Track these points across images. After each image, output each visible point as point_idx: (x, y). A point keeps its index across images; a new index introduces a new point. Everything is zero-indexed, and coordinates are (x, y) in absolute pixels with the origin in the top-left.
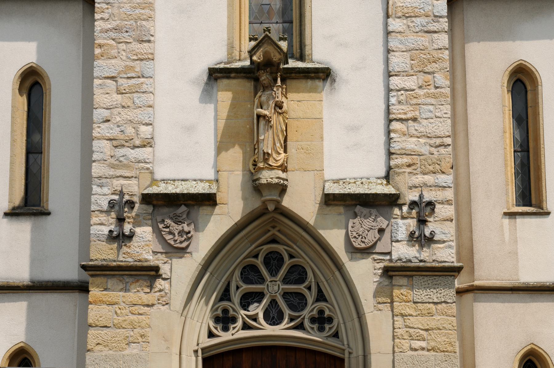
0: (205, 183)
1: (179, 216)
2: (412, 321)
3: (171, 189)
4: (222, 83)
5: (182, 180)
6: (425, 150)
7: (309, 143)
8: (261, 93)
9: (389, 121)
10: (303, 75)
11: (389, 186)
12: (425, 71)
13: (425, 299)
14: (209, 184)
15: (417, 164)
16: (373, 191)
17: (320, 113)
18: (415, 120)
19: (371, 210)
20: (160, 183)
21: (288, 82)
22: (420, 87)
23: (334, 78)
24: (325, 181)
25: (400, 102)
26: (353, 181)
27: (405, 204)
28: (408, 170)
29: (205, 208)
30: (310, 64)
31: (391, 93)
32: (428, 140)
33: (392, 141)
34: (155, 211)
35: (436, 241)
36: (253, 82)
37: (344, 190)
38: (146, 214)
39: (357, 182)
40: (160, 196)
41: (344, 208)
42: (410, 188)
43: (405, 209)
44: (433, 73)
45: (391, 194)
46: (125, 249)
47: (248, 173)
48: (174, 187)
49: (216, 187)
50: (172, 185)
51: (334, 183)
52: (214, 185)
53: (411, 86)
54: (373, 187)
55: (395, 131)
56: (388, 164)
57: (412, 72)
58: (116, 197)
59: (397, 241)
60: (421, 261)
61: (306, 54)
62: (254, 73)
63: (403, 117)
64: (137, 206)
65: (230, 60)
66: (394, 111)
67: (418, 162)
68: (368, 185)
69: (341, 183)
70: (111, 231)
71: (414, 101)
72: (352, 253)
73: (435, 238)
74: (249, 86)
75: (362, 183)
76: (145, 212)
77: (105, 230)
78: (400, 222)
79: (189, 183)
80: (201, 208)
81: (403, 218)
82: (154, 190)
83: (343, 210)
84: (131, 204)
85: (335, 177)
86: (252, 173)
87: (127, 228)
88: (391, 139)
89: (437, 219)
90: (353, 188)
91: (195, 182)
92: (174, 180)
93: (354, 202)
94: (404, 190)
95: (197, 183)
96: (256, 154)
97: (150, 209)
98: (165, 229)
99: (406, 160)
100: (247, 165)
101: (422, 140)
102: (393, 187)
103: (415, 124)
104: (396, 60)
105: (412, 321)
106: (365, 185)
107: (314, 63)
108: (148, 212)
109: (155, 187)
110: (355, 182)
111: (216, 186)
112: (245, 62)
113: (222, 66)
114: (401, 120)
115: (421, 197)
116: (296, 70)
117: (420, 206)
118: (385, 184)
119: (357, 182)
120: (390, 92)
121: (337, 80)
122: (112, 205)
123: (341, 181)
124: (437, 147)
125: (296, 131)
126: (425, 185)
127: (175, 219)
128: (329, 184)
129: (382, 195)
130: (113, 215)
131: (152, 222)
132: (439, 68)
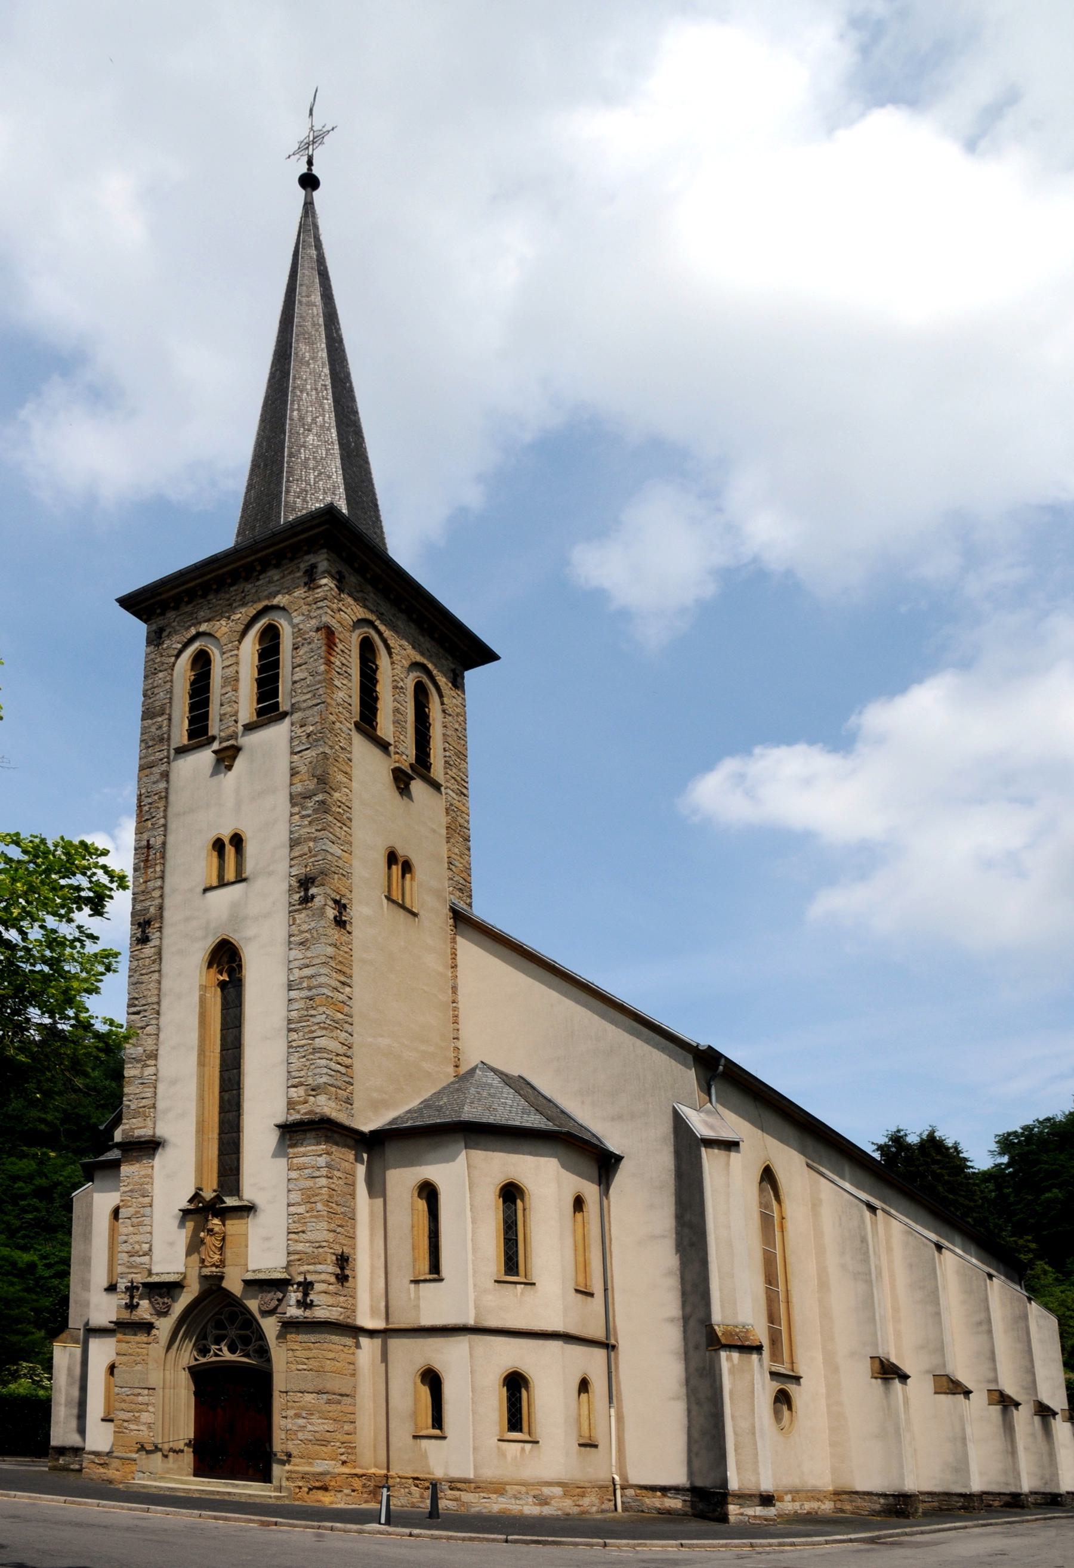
2: (298, 1353)
5: (168, 1273)
6: (309, 1250)
13: (306, 1340)
18: (303, 1232)
22: (307, 1212)
25: (294, 1222)
27: (294, 1284)
28: (299, 1263)
32: (311, 1244)
42: (299, 1274)
43: (295, 1286)
44: (316, 1203)
46: (134, 1313)
57: (302, 1203)
58: (129, 1284)
59: (290, 1306)
60: (305, 1318)
63: (296, 1231)
64: (141, 1289)
70: (126, 1303)
71: (303, 1221)
73: (314, 1304)
78: (293, 1294)
81: (295, 1292)
84: (137, 1288)
85: (255, 1269)
87: (135, 1300)
94: (294, 1274)
97: (148, 1290)
99: (297, 1257)
101: (307, 1245)
103: (304, 1235)
105: (298, 1353)
114: (294, 1233)
122: (127, 1288)
124: (317, 1248)
126: (309, 1272)
130: (128, 1294)
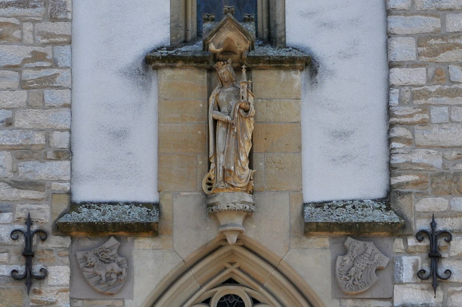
0: (142, 207)
1: (107, 252)
3: (96, 216)
4: (164, 75)
7: (282, 155)
8: (219, 89)
9: (389, 125)
10: (274, 65)
11: (390, 211)
12: (437, 61)
14: (147, 209)
15: (427, 182)
16: (370, 219)
17: (297, 115)
19: (366, 243)
20: (81, 207)
21: (254, 73)
23: (316, 68)
24: (305, 205)
26: (342, 205)
29: (141, 240)
30: (283, 50)
31: (392, 90)
33: (394, 151)
34: (74, 245)
35: (453, 283)
36: (206, 73)
37: (330, 217)
38: (62, 249)
39: (346, 207)
40: (82, 226)
41: (329, 240)
45: (393, 223)
47: (200, 194)
48: (101, 213)
49: (158, 214)
50: (98, 211)
51: (317, 207)
52: (154, 209)
53: (419, 80)
54: (368, 213)
55: (398, 139)
56: (388, 182)
61: (277, 36)
62: (208, 63)
63: (408, 120)
65: (175, 43)
66: (396, 113)
67: (427, 180)
68: (362, 210)
69: (326, 207)
72: (341, 300)
74: (202, 79)
75: (354, 207)
76: (60, 246)
77: (6, 271)
79: (120, 207)
80: (136, 241)
82: (73, 217)
83: (329, 244)
86: (206, 196)
88: (392, 149)
89: (453, 254)
90: (342, 214)
91: (127, 206)
92: (99, 204)
93: (343, 233)
95: (131, 207)
96: (213, 170)
98: (87, 269)
100: (198, 183)
102: (395, 213)
104: (398, 46)
106: (357, 210)
107: (288, 48)
108: (65, 247)
109: (74, 213)
110: (344, 207)
111: (157, 212)
112: (195, 46)
113: (165, 52)
115: (433, 225)
116: (265, 59)
117: (431, 237)
118: (384, 209)
119: (346, 207)
120: (391, 88)
121: (320, 70)
123: (326, 204)
125: (266, 139)
127: (102, 255)
128: (309, 208)
129: (381, 224)
131: (70, 259)
132: (455, 57)
